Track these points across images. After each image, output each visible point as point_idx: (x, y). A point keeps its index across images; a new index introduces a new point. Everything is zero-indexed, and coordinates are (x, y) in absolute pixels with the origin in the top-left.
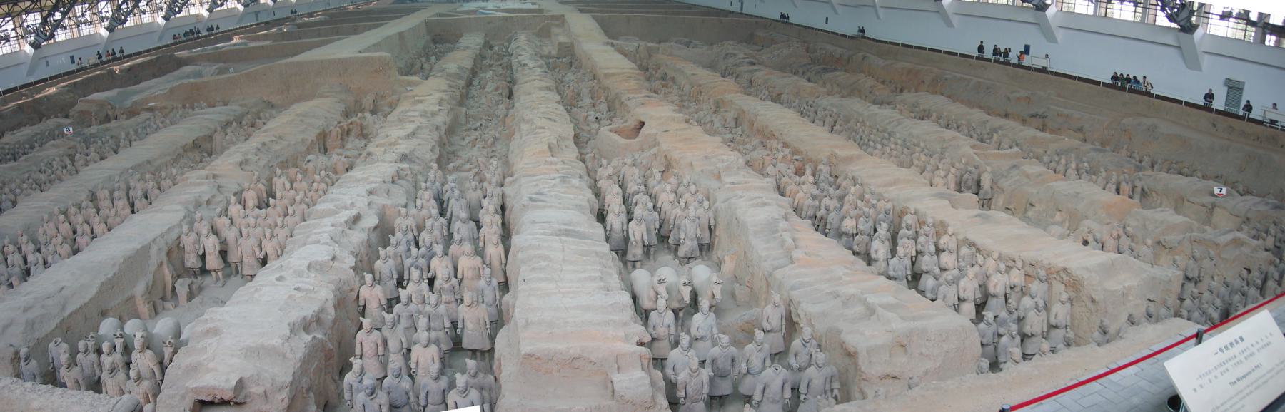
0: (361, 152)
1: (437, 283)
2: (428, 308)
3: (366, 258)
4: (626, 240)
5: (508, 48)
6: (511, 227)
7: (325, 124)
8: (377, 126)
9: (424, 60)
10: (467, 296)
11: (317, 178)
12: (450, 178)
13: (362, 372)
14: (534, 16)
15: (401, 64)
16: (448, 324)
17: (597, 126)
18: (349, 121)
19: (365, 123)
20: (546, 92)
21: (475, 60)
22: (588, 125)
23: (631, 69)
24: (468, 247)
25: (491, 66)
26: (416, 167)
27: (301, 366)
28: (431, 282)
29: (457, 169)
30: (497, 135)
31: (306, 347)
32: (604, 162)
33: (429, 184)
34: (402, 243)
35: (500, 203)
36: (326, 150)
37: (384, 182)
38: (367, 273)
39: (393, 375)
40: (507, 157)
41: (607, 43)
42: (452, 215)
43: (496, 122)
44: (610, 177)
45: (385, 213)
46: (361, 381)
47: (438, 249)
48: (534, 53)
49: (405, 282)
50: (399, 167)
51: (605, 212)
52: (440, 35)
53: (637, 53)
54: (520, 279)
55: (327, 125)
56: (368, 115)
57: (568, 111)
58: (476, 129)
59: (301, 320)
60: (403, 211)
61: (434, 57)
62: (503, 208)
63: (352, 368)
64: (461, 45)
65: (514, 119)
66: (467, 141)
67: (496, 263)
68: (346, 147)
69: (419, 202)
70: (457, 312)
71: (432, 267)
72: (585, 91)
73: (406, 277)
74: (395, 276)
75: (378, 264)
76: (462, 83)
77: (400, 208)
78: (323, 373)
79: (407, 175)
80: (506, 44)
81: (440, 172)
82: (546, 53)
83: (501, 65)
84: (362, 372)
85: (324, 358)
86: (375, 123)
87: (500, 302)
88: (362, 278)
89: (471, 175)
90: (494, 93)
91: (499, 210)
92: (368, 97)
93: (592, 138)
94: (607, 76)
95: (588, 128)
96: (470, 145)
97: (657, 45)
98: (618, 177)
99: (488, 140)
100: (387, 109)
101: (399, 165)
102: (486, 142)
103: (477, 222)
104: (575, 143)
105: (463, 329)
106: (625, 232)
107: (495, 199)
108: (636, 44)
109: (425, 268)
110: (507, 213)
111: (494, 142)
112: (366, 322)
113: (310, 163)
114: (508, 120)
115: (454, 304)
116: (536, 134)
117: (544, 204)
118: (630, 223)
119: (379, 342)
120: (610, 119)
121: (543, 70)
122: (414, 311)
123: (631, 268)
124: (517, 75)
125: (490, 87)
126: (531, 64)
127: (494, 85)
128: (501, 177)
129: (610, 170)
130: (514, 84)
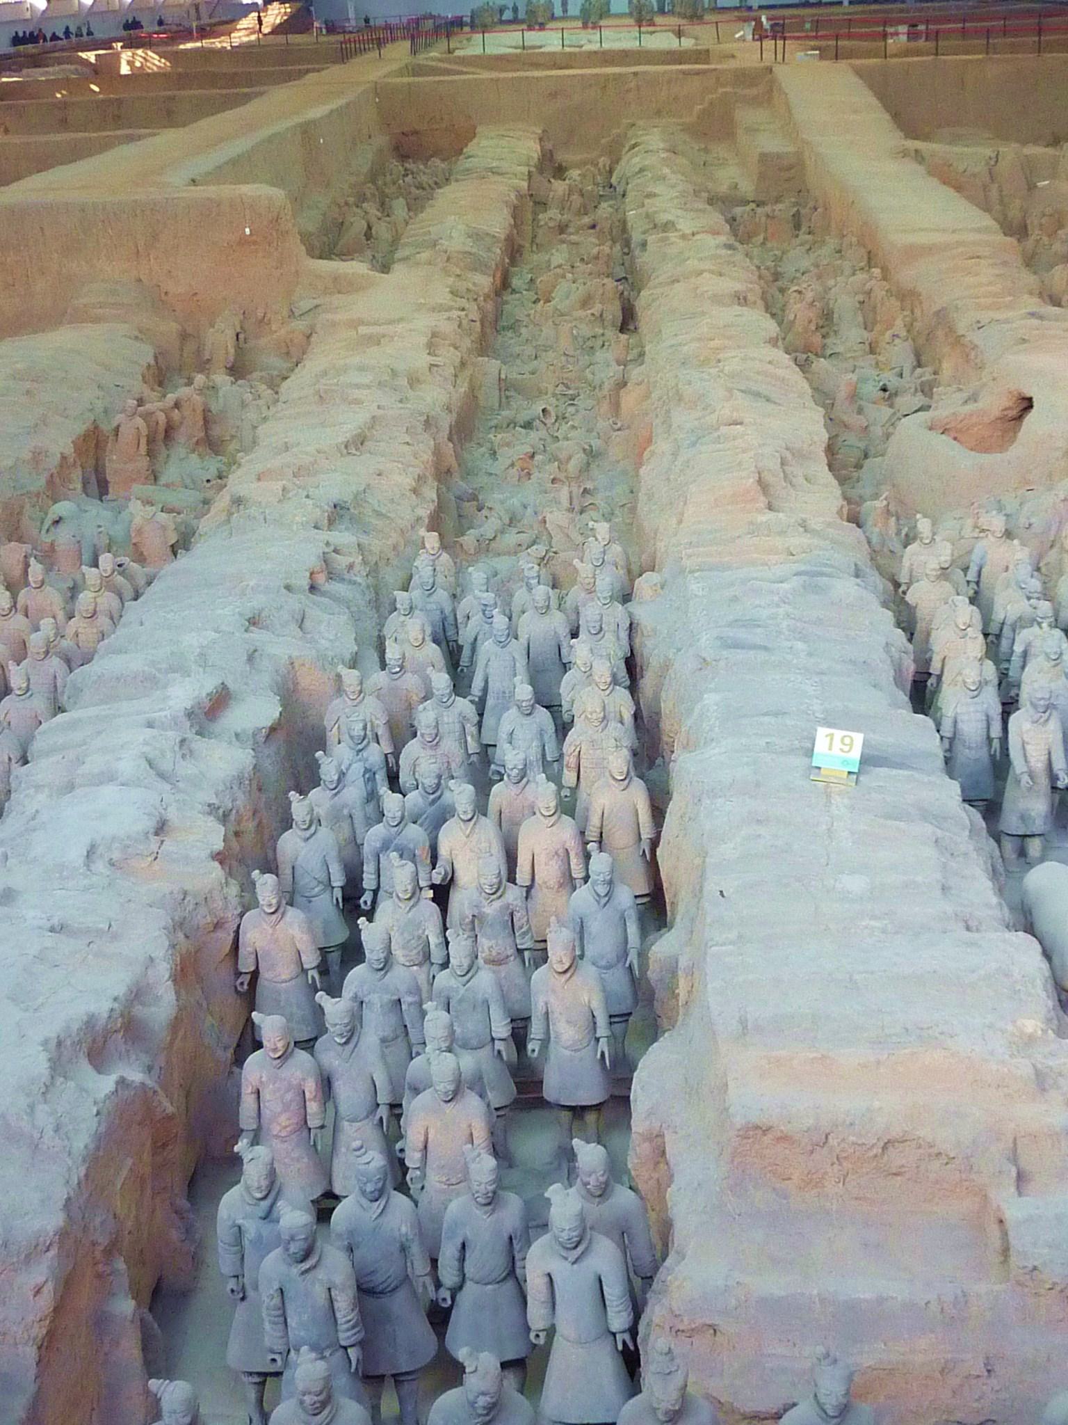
0: (209, 494)
1: (460, 901)
2: (443, 978)
3: (250, 826)
4: (1000, 765)
5: (611, 172)
6: (666, 725)
7: (99, 405)
8: (251, 415)
9: (372, 208)
10: (559, 945)
11: (91, 574)
12: (477, 575)
13: (272, 1189)
14: (684, 73)
15: (311, 222)
16: (501, 1029)
17: (886, 412)
18: (171, 397)
19: (214, 407)
20: (737, 309)
21: (516, 212)
22: (860, 411)
23: (979, 230)
24: (543, 792)
25: (562, 228)
26: (376, 544)
27: (87, 1176)
28: (442, 894)
29: (485, 547)
30: (596, 443)
31: (98, 1114)
32: (924, 525)
33: (416, 594)
34: (351, 776)
35: (623, 651)
36: (103, 488)
37: (288, 588)
38: (263, 872)
39: (363, 1193)
40: (633, 510)
41: (905, 153)
42: (485, 690)
43: (590, 403)
44: (944, 573)
45: (296, 684)
46: (268, 1216)
47: (461, 794)
48: (690, 188)
49: (367, 897)
50: (328, 544)
51: (932, 681)
52: (416, 133)
53: (992, 179)
54: (711, 887)
55: (106, 411)
56: (221, 378)
57: (804, 366)
58: (528, 425)
59: (80, 1029)
60: (351, 677)
61: (401, 201)
62: (632, 666)
63: (241, 1172)
64: (468, 164)
65: (647, 396)
66: (509, 462)
67: (621, 837)
68: (163, 480)
69: (392, 653)
70: (527, 995)
71: (443, 851)
72: (844, 303)
73: (368, 882)
74: (338, 880)
75: (290, 844)
76: (484, 282)
77: (342, 670)
78: (149, 1192)
79: (351, 567)
80: (604, 161)
81: (445, 557)
82: (723, 189)
83: (593, 227)
84: (272, 1189)
85: (149, 1143)
86: (244, 405)
87: (643, 955)
88: (249, 887)
89: (528, 565)
90: (581, 313)
91: (623, 673)
92: (220, 325)
93: (872, 451)
94: (913, 253)
95: (861, 421)
96: (514, 471)
97: (1050, 151)
98: (966, 570)
99: (570, 458)
100: (276, 363)
101: (325, 535)
102: (562, 463)
103: (553, 707)
104: (831, 467)
105: (546, 1042)
106: (996, 744)
107: (609, 637)
108: (988, 152)
109: (423, 854)
110: (647, 683)
111: (588, 464)
112: (270, 1025)
113: (61, 526)
114: (629, 399)
115: (513, 966)
116: (718, 440)
117: (762, 656)
118: (1013, 719)
119: (310, 1087)
120: (926, 389)
121: (723, 239)
122: (403, 988)
123: (1014, 856)
124: (644, 259)
125: (566, 293)
126: (685, 226)
127: (579, 291)
128: (622, 572)
129: (944, 553)
130: (637, 288)
